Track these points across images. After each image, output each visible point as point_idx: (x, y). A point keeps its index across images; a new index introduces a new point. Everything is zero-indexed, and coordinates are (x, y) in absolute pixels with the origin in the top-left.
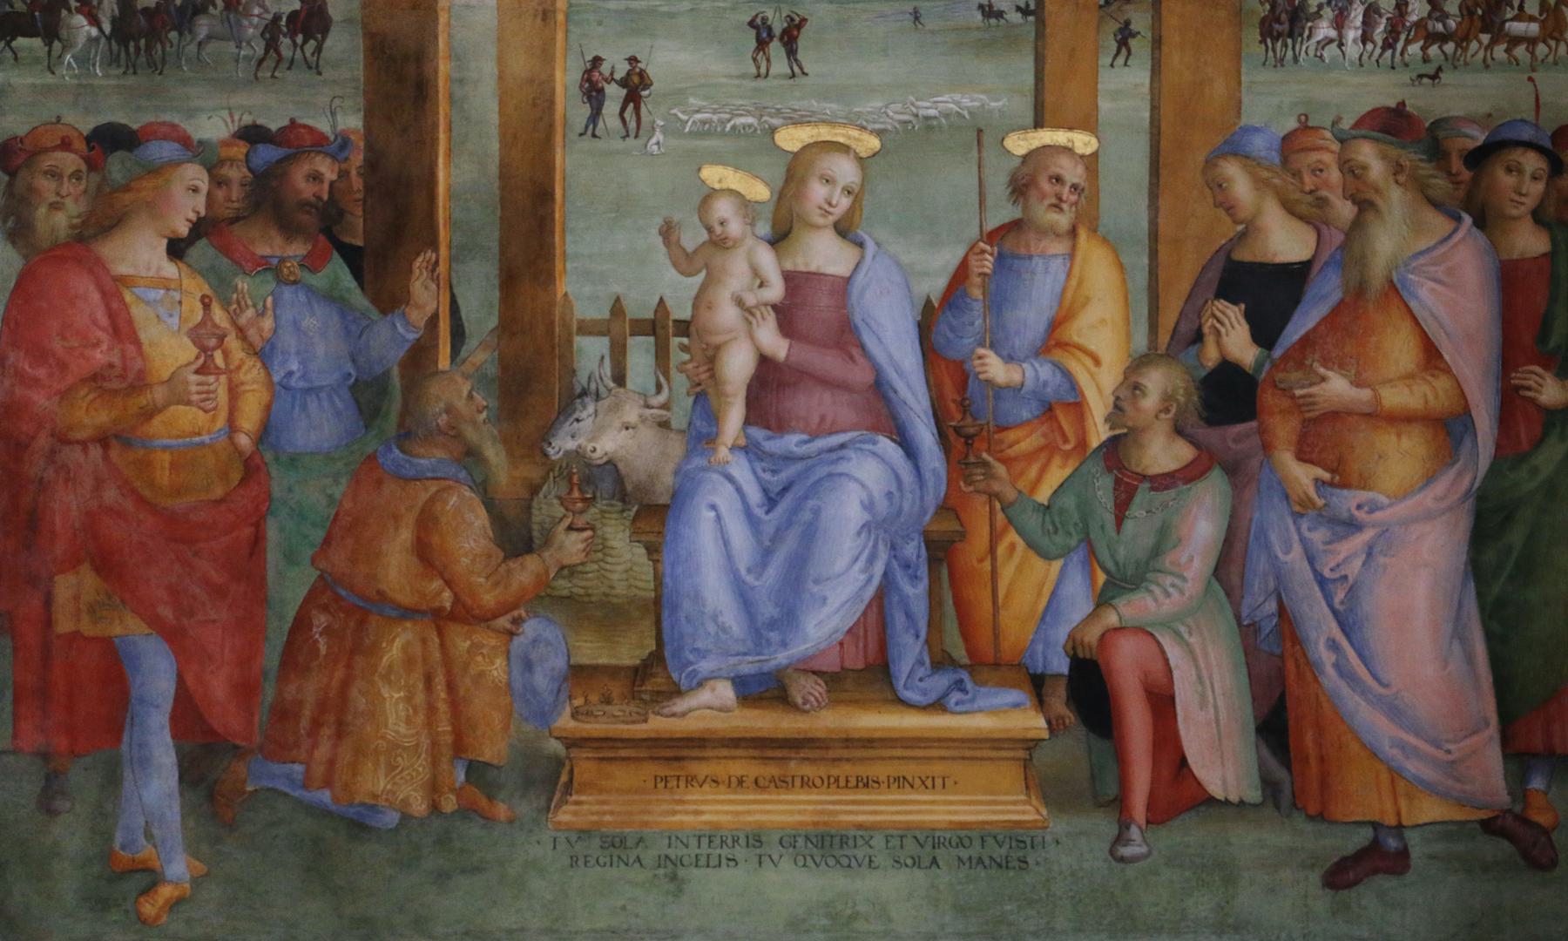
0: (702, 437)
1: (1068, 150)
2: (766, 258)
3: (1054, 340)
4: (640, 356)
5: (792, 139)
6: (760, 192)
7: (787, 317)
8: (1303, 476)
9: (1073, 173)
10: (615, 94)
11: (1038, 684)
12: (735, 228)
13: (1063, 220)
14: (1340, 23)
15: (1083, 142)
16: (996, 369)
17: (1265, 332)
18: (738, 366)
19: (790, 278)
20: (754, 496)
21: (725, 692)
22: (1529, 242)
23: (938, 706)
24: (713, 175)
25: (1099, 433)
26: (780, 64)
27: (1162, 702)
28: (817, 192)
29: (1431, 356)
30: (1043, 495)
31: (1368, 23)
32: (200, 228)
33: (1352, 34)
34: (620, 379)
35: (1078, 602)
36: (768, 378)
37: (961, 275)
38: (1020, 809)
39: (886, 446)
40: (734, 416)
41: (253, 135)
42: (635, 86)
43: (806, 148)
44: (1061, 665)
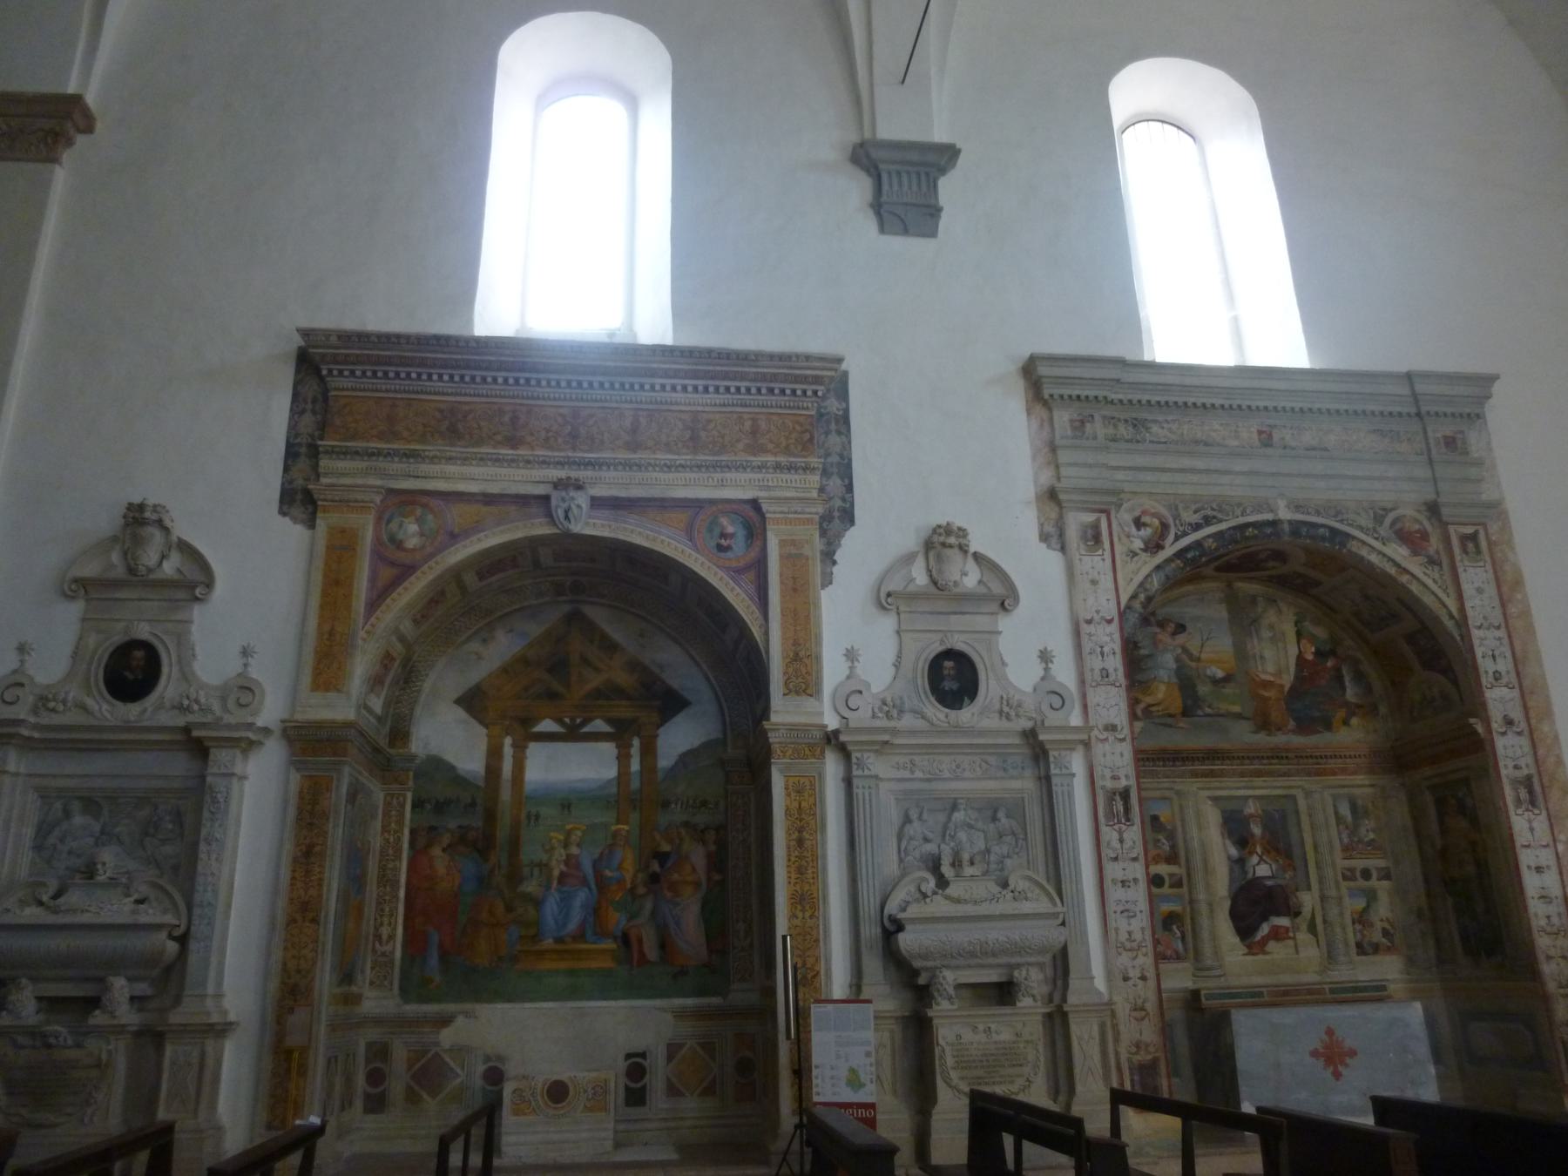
0: (548, 888)
1: (623, 829)
2: (562, 851)
3: (620, 868)
4: (536, 871)
5: (568, 827)
6: (562, 837)
7: (567, 863)
8: (669, 895)
9: (624, 833)
10: (533, 818)
11: (615, 938)
12: (556, 845)
13: (622, 843)
14: (676, 804)
15: (626, 827)
16: (608, 873)
17: (662, 866)
18: (556, 873)
19: (568, 856)
20: (558, 899)
21: (551, 941)
22: (713, 848)
23: (595, 943)
24: (552, 834)
25: (629, 886)
26: (566, 812)
27: (640, 941)
28: (574, 837)
29: (694, 869)
30: (617, 899)
31: (682, 804)
32: (449, 846)
33: (679, 806)
34: (532, 875)
35: (624, 922)
36: (563, 876)
37: (602, 854)
38: (608, 963)
39: (586, 890)
40: (555, 882)
41: (460, 827)
42: (537, 817)
43: (571, 829)
44: (619, 934)
